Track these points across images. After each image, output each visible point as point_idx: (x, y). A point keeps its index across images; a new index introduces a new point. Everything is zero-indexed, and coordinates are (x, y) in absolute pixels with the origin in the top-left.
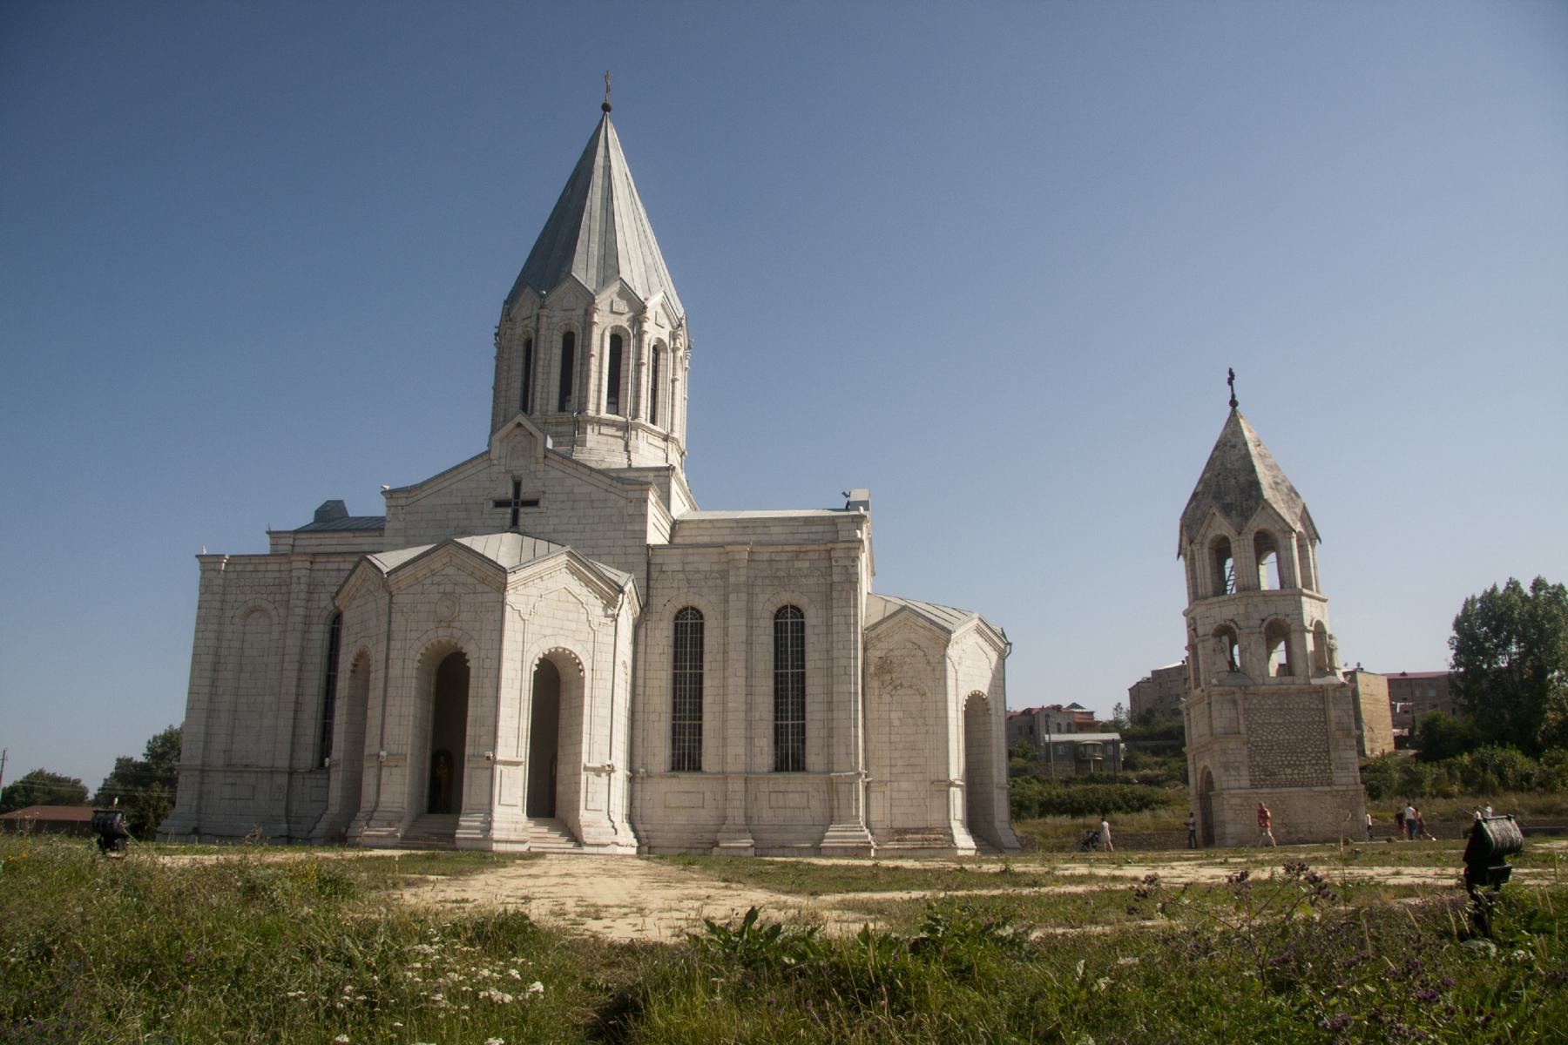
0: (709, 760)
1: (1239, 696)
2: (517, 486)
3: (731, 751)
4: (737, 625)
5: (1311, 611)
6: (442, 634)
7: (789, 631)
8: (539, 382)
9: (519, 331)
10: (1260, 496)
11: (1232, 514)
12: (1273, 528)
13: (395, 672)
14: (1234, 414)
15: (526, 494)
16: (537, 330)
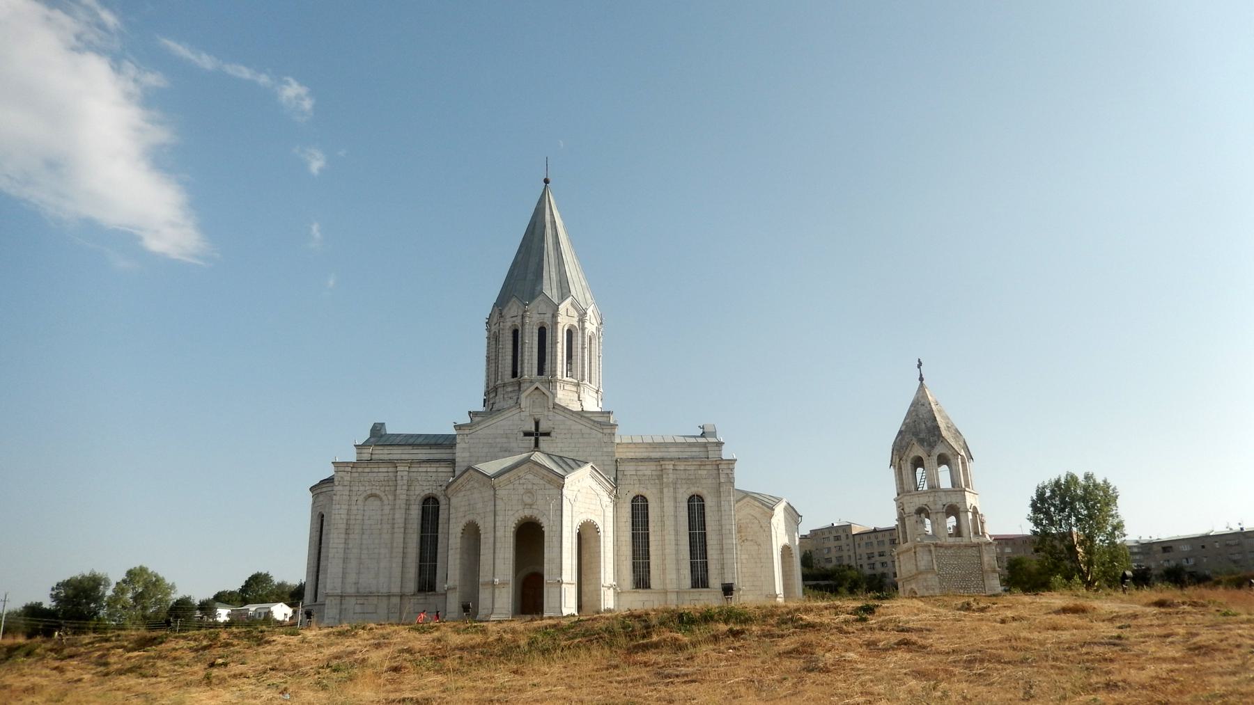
0: (654, 582)
1: (932, 548)
2: (537, 424)
3: (668, 577)
4: (669, 505)
5: (970, 500)
6: (527, 513)
7: (696, 507)
8: (526, 357)
9: (509, 324)
10: (940, 435)
11: (922, 440)
12: (949, 453)
13: (499, 534)
14: (922, 385)
15: (543, 428)
16: (523, 325)
